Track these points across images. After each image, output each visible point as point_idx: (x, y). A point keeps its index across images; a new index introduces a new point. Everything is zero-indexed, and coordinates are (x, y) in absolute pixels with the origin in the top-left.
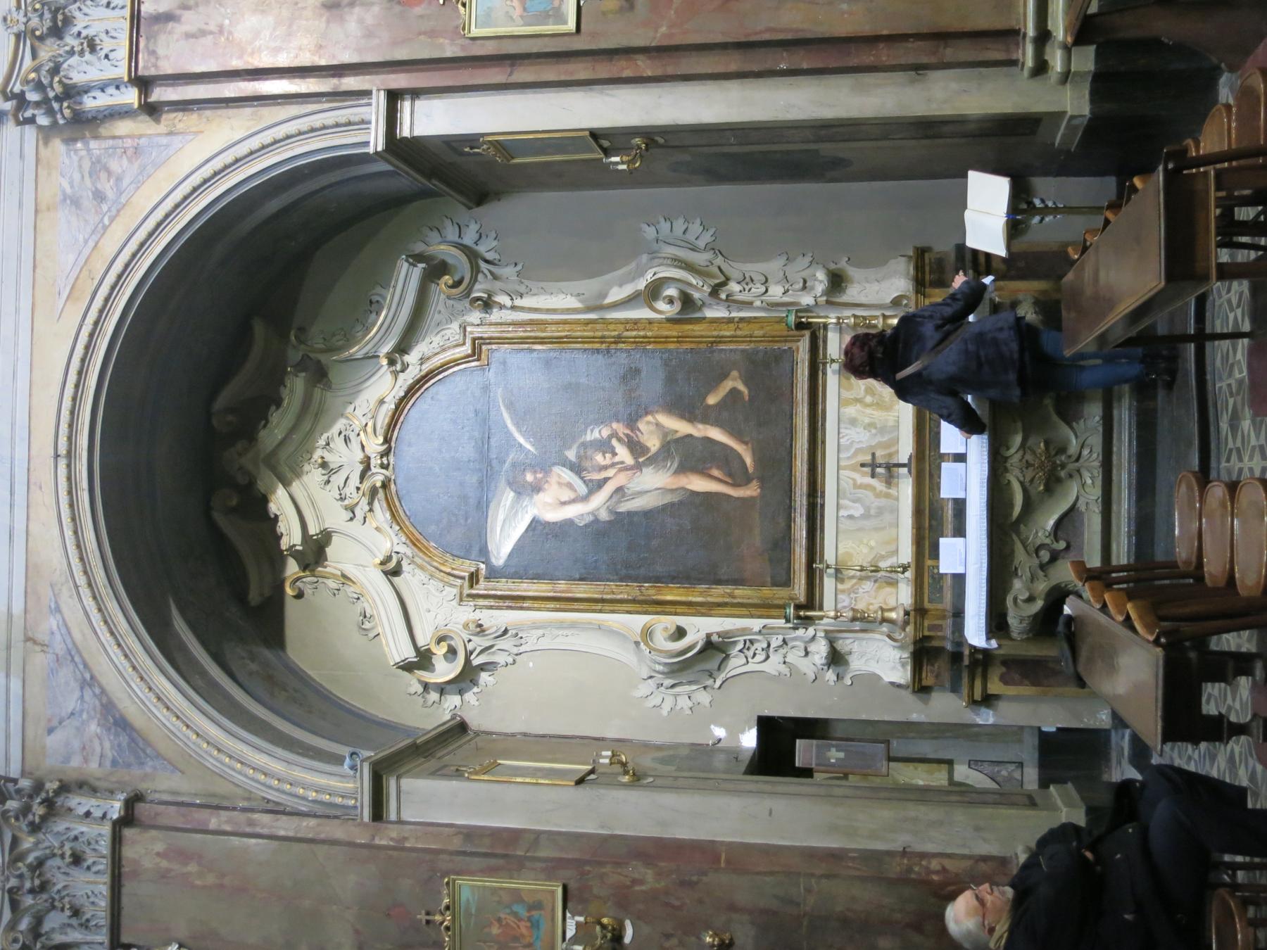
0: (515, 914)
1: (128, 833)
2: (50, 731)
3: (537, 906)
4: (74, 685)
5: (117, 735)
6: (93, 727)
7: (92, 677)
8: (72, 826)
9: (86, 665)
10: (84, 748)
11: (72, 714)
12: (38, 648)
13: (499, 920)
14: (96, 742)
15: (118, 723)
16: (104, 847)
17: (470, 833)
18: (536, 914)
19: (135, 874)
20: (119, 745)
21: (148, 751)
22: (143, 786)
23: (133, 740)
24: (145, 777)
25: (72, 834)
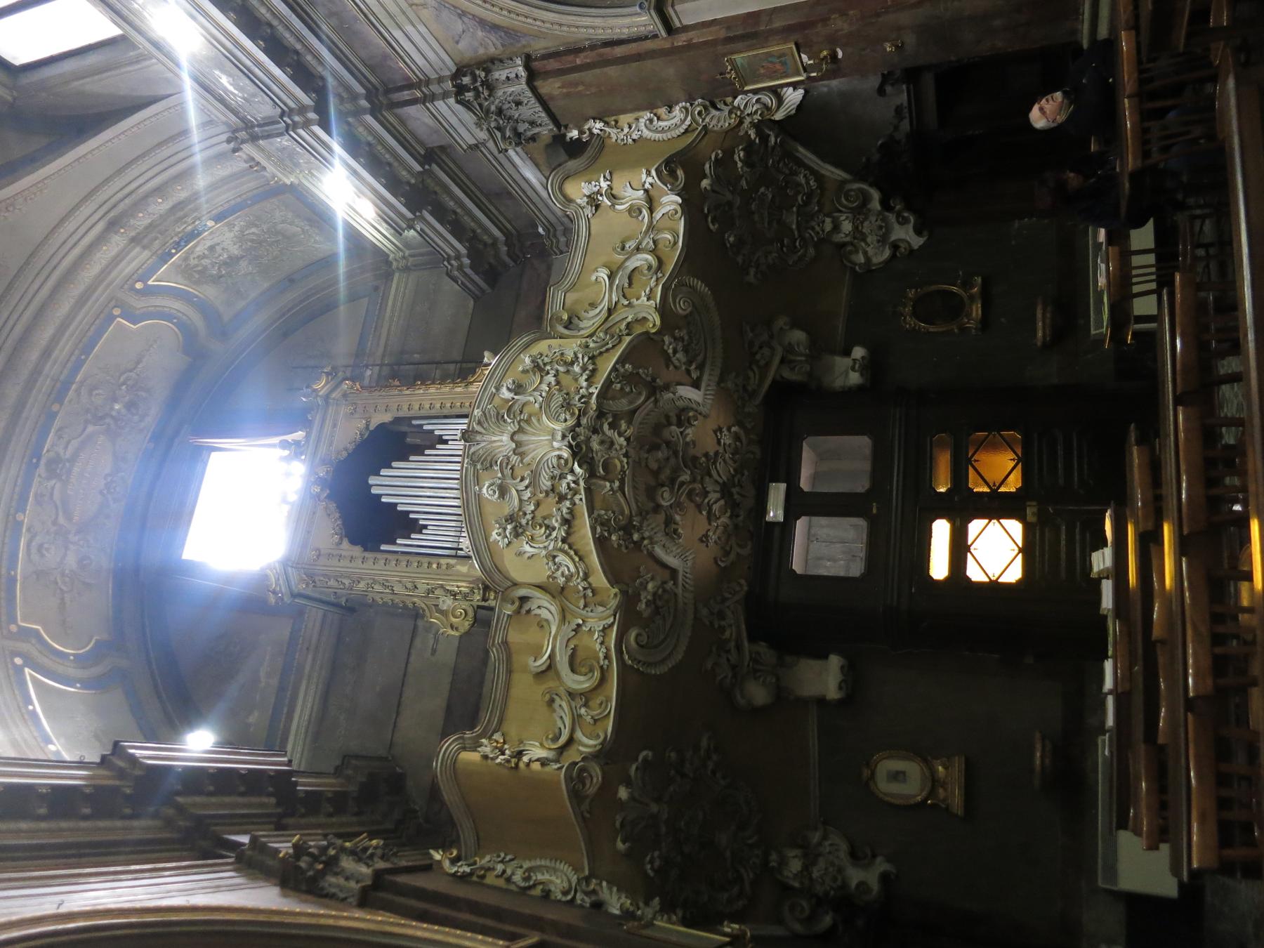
0: (771, 62)
1: (538, 83)
2: (457, 42)
3: (782, 55)
4: (457, 18)
5: (496, 33)
6: (480, 34)
7: (462, 11)
8: (506, 90)
9: (453, 6)
10: (481, 44)
11: (464, 31)
12: (420, 7)
13: (763, 67)
14: (486, 39)
15: (495, 27)
16: (529, 94)
17: (727, 22)
18: (783, 59)
19: (552, 98)
20: (501, 37)
21: (519, 34)
22: (526, 50)
23: (506, 33)
24: (524, 46)
25: (508, 93)
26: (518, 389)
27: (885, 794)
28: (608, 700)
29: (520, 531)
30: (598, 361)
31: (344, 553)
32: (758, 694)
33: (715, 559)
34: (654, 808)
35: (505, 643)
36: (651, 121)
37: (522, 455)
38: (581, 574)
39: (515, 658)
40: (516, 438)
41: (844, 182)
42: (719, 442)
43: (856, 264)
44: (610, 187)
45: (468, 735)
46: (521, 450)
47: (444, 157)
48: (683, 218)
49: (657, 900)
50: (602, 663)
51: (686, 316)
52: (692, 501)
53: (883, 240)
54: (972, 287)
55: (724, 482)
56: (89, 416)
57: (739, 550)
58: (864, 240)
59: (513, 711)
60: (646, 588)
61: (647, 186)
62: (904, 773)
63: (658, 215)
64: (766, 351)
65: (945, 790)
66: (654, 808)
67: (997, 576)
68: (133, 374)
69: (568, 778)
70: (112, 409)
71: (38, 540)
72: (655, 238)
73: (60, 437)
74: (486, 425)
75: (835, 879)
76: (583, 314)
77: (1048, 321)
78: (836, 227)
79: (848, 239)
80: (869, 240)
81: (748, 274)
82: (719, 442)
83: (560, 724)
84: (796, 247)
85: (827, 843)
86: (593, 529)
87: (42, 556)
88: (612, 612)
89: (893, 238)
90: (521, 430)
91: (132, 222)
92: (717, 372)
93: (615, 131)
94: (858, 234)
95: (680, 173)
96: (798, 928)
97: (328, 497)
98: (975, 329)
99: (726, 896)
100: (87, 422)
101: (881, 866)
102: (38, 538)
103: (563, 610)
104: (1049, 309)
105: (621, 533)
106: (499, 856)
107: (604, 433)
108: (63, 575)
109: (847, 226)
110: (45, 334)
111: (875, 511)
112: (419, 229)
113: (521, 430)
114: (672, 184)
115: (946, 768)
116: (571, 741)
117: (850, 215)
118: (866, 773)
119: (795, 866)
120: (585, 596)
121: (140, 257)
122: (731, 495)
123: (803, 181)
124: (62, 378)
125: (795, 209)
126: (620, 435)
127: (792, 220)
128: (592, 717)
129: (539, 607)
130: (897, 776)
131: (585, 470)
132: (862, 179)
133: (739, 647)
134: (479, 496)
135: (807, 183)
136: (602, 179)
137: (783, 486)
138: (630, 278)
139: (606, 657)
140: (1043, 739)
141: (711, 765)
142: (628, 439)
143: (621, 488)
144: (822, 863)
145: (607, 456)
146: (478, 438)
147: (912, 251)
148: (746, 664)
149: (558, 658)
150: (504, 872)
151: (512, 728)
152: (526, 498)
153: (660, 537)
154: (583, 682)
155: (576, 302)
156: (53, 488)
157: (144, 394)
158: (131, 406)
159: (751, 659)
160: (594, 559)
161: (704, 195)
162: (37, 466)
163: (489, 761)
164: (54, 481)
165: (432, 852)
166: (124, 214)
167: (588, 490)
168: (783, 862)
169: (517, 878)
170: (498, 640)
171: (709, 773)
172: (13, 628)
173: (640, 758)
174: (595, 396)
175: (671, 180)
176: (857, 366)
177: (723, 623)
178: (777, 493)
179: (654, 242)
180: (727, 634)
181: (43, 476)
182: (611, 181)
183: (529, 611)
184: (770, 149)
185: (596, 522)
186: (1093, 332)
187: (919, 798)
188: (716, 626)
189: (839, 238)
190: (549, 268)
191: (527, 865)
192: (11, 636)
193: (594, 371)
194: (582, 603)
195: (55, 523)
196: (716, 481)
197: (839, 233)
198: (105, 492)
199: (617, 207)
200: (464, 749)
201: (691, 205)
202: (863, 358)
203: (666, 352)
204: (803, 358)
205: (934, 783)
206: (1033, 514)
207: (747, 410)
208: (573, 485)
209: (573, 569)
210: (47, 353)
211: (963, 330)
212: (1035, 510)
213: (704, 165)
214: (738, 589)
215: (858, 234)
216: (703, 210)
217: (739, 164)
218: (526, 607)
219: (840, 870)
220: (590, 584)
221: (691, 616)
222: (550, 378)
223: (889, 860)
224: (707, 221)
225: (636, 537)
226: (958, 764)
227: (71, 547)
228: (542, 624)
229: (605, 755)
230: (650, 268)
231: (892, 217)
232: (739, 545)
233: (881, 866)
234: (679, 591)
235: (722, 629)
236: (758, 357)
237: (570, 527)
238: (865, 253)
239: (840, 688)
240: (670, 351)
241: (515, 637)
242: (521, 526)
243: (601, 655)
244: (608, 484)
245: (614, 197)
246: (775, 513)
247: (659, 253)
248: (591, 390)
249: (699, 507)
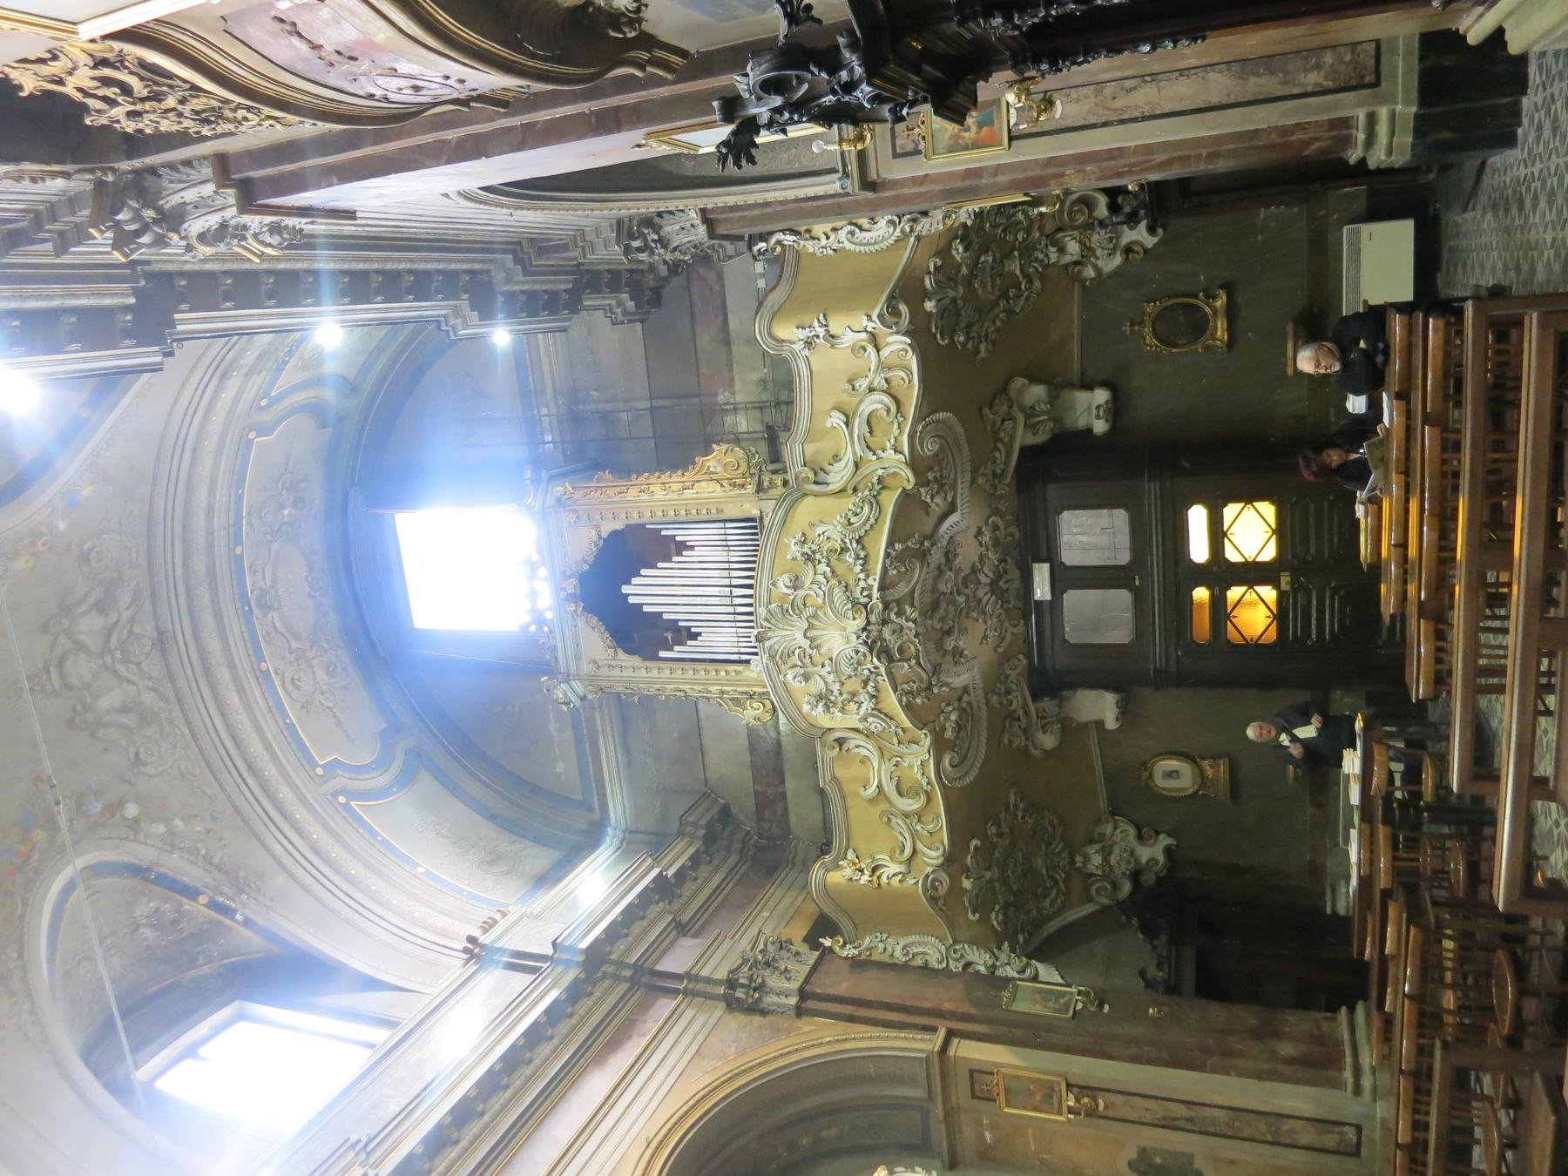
26: (796, 584)
28: (938, 816)
30: (866, 541)
31: (624, 664)
32: (1048, 741)
34: (988, 875)
35: (834, 778)
36: (852, 233)
37: (818, 647)
39: (845, 786)
40: (809, 634)
42: (981, 544)
44: (827, 331)
45: (827, 858)
46: (815, 643)
49: (1006, 944)
50: (925, 788)
56: (268, 537)
57: (1014, 630)
59: (856, 829)
61: (869, 329)
62: (1177, 772)
64: (1008, 424)
68: (288, 476)
69: (925, 889)
70: (283, 517)
71: (288, 676)
73: (255, 572)
74: (773, 621)
75: (1129, 863)
76: (828, 468)
80: (1099, 252)
83: (901, 838)
85: (1118, 831)
87: (298, 688)
88: (926, 750)
89: (1124, 241)
90: (811, 627)
91: (242, 362)
93: (811, 242)
94: (1087, 250)
95: (903, 308)
96: (1104, 901)
97: (584, 609)
99: (1048, 900)
100: (269, 543)
101: (1165, 841)
102: (286, 675)
103: (880, 748)
106: (877, 937)
107: (892, 622)
108: (323, 693)
109: (1073, 248)
110: (202, 494)
111: (1137, 583)
113: (811, 627)
114: (897, 324)
116: (915, 851)
118: (1145, 775)
119: (1097, 860)
120: (896, 734)
121: (257, 382)
124: (231, 522)
125: (1016, 253)
126: (908, 620)
129: (857, 747)
133: (1027, 713)
134: (785, 684)
136: (816, 324)
137: (1046, 566)
138: (869, 423)
139: (928, 784)
141: (1020, 814)
142: (915, 621)
143: (919, 663)
144: (1116, 850)
145: (899, 642)
146: (770, 634)
147: (1146, 251)
149: (886, 789)
150: (885, 949)
151: (860, 843)
154: (910, 805)
155: (817, 452)
156: (273, 622)
157: (303, 485)
158: (297, 503)
159: (1038, 717)
162: (250, 609)
163: (854, 883)
164: (270, 616)
165: (821, 940)
166: (234, 360)
167: (890, 674)
168: (1087, 859)
169: (898, 953)
170: (828, 777)
172: (319, 771)
173: (972, 848)
174: (875, 589)
175: (896, 320)
176: (1101, 412)
178: (1041, 579)
179: (886, 380)
180: (1014, 706)
181: (259, 616)
182: (826, 326)
187: (1191, 791)
190: (720, 277)
191: (902, 942)
192: (324, 780)
193: (866, 559)
194: (895, 741)
195: (291, 652)
198: (312, 593)
200: (827, 871)
201: (919, 335)
202: (1107, 402)
206: (1287, 583)
207: (998, 493)
210: (210, 513)
212: (1288, 579)
213: (923, 281)
214: (1017, 663)
215: (1087, 250)
216: (930, 330)
218: (845, 748)
219: (1132, 853)
222: (822, 568)
223: (1169, 835)
224: (936, 338)
227: (315, 662)
228: (864, 761)
229: (951, 861)
230: (888, 411)
233: (1165, 841)
235: (1011, 703)
236: (1002, 434)
239: (1117, 719)
240: (929, 500)
241: (839, 772)
245: (832, 336)
246: (1042, 591)
247: (893, 391)
248: (870, 581)
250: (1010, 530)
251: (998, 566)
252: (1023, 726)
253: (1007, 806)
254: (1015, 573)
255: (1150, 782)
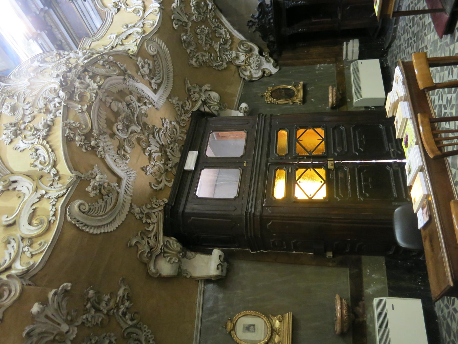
27: (240, 340)
29: (19, 132)
33: (150, 184)
34: (65, 328)
38: (51, 161)
41: (243, 41)
43: (245, 76)
47: (58, 9)
48: (159, 14)
51: (153, 56)
52: (139, 144)
53: (259, 66)
54: (298, 86)
55: (163, 145)
58: (250, 65)
60: (94, 178)
63: (147, 13)
65: (279, 336)
66: (65, 328)
67: (312, 195)
72: (144, 23)
77: (334, 93)
78: (237, 57)
79: (242, 64)
80: (252, 66)
81: (192, 60)
82: (163, 124)
84: (218, 60)
86: (64, 131)
89: (263, 67)
92: (168, 93)
98: (300, 101)
104: (335, 88)
105: (83, 137)
112: (40, 43)
115: (280, 321)
117: (244, 54)
118: (230, 326)
122: (166, 152)
123: (224, 33)
127: (217, 47)
128: (31, 253)
130: (249, 328)
131: (66, 93)
132: (252, 41)
133: (156, 237)
135: (226, 34)
139: (54, 215)
140: (341, 299)
141: (122, 308)
147: (271, 75)
148: (160, 247)
152: (27, 113)
153: (113, 152)
160: (60, 152)
161: (173, 11)
171: (120, 313)
177: (149, 221)
178: (192, 157)
179: (143, 24)
180: (151, 228)
183: (14, 189)
184: (209, 10)
185: (66, 126)
186: (355, 100)
188: (144, 221)
189: (237, 62)
196: (158, 142)
197: (239, 60)
199: (128, 9)
203: (138, 65)
204: (216, 103)
205: (273, 331)
208: (57, 105)
209: (47, 159)
211: (294, 103)
217: (193, 8)
220: (58, 172)
221: (127, 209)
225: (93, 143)
226: (288, 318)
231: (263, 59)
232: (166, 180)
234: (122, 192)
237: (49, 130)
238: (250, 72)
239: (218, 268)
240: (140, 65)
242: (20, 130)
243: (52, 213)
244: (80, 106)
245: (127, 4)
246: (190, 165)
249: (144, 150)
250: (182, 135)
251: (169, 145)
252: (151, 244)
253: (113, 294)
254: (179, 155)
255: (233, 333)
